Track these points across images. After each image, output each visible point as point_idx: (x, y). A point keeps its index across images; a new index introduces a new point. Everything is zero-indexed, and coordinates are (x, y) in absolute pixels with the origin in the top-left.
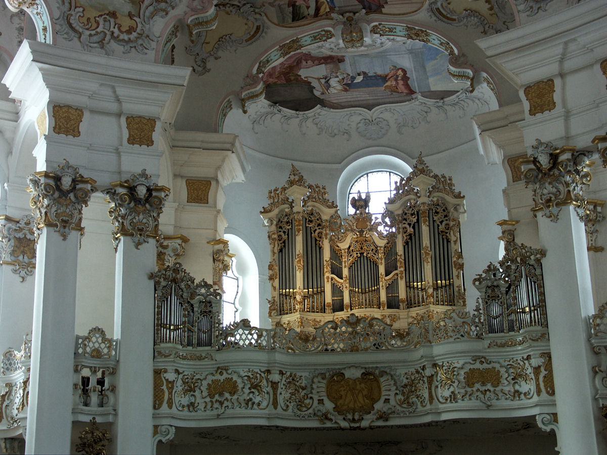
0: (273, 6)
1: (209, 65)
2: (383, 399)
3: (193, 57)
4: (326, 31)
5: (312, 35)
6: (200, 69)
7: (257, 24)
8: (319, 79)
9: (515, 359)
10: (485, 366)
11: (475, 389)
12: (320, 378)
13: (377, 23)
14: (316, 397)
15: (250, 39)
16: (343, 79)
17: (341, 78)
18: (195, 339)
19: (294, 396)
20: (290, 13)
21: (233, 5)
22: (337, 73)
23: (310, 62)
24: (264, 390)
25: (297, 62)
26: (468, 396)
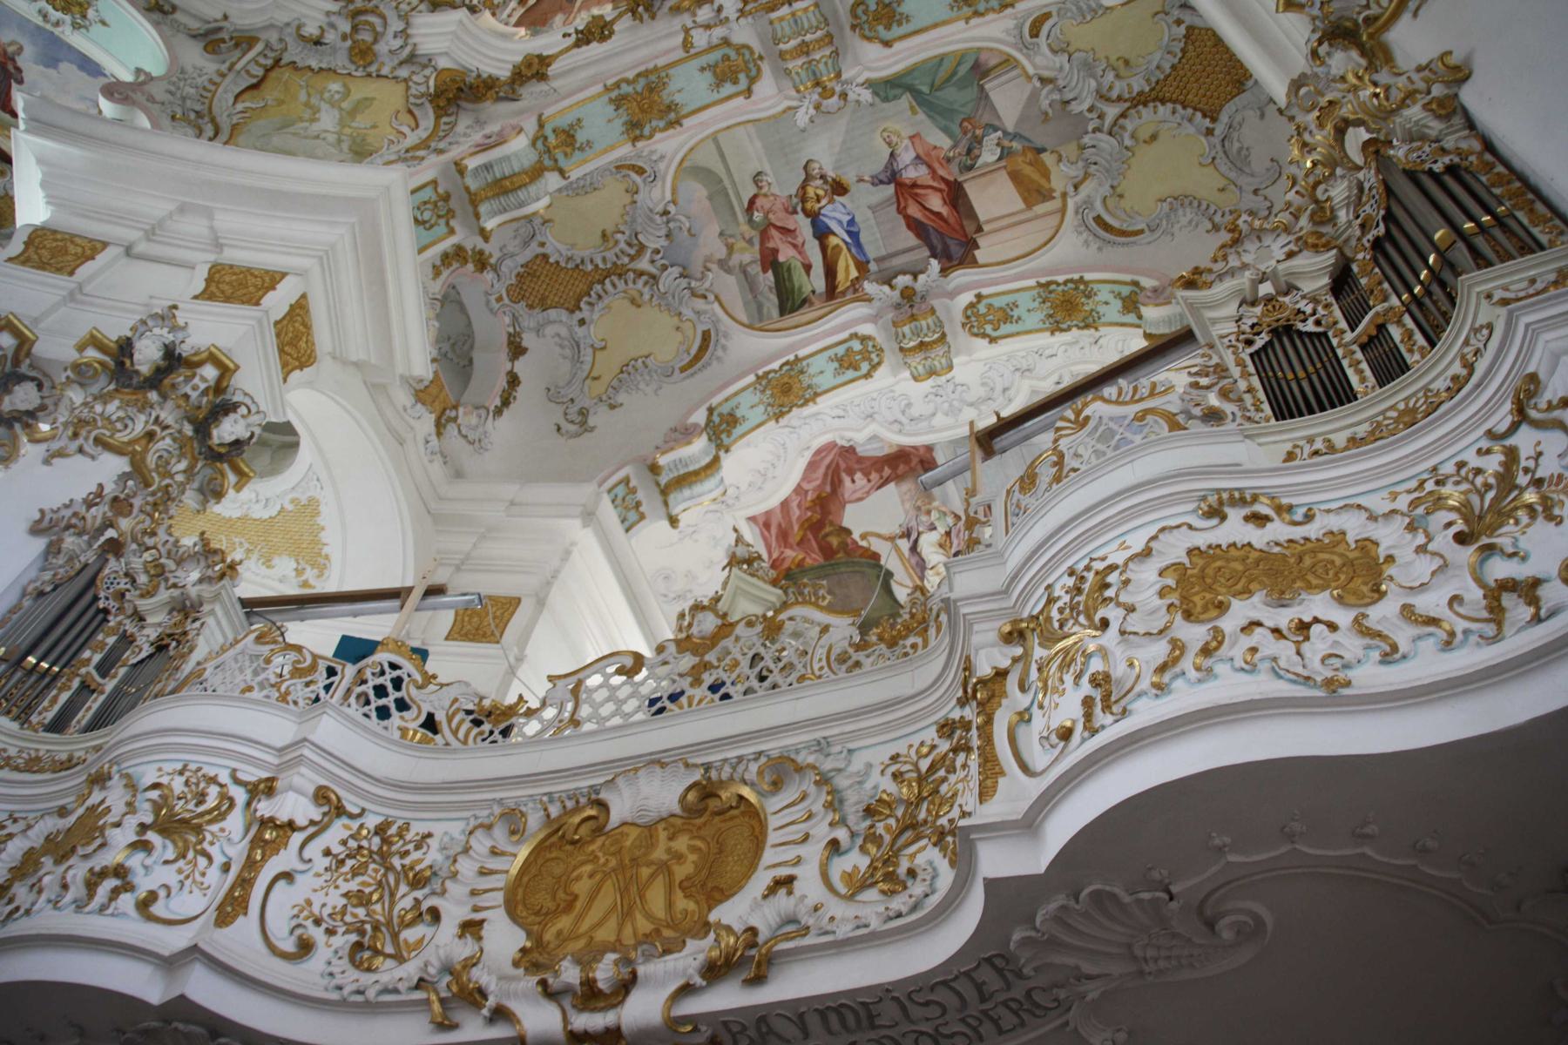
0: (729, 271)
1: (591, 421)
2: (762, 880)
3: (561, 409)
4: (864, 339)
5: (831, 352)
6: (572, 428)
7: (701, 328)
8: (891, 539)
9: (1449, 468)
10: (1278, 530)
11: (1230, 623)
12: (500, 834)
13: (967, 298)
14: (454, 911)
15: (692, 364)
16: (948, 534)
17: (943, 532)
18: (87, 710)
19: (361, 912)
20: (770, 288)
21: (641, 274)
22: (929, 513)
23: (858, 476)
24: (214, 851)
25: (833, 483)
26: (1187, 664)
